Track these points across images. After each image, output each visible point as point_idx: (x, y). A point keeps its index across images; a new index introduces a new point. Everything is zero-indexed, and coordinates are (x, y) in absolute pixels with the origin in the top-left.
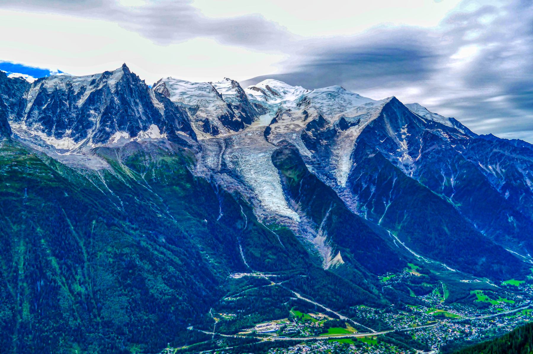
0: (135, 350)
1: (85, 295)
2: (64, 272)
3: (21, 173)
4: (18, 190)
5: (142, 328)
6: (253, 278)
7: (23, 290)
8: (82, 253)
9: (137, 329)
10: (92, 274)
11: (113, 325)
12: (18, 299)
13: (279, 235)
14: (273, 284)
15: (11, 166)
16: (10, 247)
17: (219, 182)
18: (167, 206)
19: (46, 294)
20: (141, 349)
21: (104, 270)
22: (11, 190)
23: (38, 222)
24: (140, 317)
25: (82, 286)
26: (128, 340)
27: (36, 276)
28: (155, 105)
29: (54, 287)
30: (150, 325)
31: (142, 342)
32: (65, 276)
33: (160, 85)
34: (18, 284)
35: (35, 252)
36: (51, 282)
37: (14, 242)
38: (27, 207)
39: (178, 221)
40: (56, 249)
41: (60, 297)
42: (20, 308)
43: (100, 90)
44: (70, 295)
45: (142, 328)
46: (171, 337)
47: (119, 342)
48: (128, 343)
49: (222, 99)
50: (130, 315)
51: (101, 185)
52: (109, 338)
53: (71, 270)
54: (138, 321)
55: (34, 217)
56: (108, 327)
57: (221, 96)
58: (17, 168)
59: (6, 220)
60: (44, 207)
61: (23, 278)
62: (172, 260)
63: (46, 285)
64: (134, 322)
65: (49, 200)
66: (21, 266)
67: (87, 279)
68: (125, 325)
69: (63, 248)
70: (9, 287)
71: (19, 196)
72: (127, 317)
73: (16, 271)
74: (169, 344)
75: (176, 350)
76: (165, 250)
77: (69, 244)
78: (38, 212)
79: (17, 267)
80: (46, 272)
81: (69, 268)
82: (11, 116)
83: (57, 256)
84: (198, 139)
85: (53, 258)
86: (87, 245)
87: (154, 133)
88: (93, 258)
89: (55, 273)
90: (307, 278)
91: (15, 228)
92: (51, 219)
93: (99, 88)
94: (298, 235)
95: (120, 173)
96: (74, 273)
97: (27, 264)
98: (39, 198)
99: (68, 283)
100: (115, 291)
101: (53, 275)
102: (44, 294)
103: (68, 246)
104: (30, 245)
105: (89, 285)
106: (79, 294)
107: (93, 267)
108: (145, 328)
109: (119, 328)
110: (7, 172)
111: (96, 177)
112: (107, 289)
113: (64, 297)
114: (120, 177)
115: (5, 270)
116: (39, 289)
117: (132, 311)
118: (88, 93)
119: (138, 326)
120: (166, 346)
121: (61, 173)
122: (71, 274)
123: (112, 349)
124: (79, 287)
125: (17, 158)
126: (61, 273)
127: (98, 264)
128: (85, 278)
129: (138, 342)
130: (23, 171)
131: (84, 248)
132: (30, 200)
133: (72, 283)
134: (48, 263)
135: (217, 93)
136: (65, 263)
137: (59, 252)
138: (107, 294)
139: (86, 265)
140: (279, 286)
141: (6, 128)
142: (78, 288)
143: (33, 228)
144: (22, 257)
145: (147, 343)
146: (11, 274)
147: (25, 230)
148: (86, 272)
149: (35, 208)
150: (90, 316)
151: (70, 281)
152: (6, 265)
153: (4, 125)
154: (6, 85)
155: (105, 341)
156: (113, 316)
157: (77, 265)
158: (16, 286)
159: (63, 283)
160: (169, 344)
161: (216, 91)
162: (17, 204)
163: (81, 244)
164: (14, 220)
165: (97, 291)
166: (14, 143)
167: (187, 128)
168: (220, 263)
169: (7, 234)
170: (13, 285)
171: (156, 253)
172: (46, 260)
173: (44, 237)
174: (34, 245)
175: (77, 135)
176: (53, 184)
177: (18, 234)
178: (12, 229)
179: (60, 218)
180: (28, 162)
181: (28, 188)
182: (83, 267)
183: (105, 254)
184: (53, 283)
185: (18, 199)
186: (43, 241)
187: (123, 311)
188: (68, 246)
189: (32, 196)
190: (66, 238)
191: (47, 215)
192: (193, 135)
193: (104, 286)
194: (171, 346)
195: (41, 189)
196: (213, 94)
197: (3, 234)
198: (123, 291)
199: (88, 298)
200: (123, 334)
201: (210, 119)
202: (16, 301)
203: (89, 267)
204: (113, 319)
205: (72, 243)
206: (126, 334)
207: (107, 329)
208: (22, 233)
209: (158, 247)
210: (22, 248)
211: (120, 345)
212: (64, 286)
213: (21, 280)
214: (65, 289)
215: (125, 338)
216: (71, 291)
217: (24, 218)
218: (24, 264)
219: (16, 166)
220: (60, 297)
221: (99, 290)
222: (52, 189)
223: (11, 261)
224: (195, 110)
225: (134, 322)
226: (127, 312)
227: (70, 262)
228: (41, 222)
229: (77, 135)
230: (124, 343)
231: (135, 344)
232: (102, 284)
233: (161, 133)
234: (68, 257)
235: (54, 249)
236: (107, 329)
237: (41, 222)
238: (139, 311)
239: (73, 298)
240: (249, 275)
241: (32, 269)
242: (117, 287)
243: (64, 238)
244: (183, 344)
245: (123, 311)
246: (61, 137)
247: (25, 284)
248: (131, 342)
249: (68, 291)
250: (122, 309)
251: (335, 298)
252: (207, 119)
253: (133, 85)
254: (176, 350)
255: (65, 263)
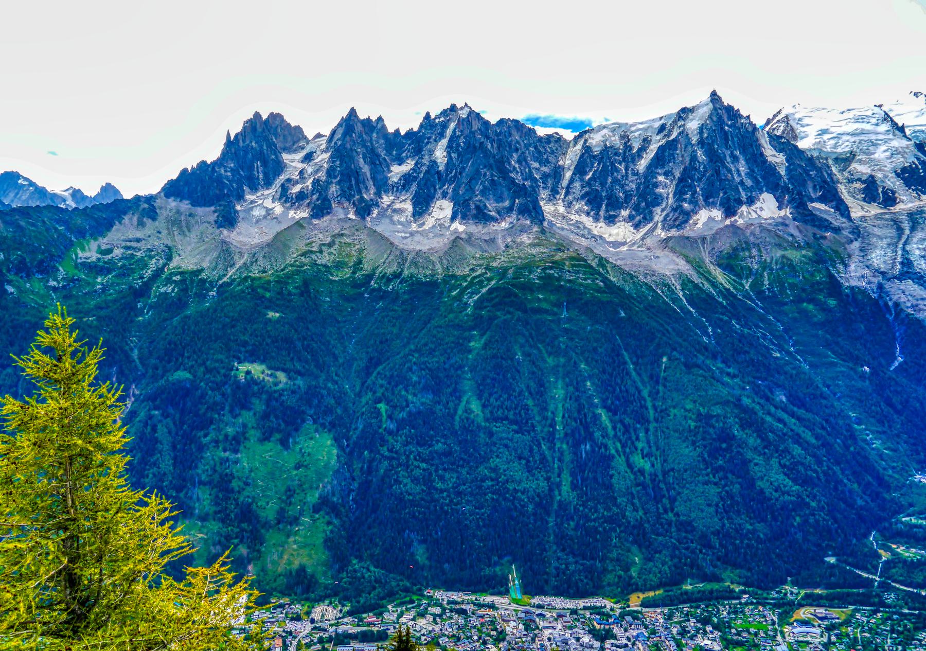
1: (650, 475)
2: (619, 434)
3: (558, 279)
4: (555, 305)
5: (742, 542)
7: (562, 454)
8: (647, 409)
9: (734, 544)
10: (662, 443)
11: (694, 529)
12: (556, 466)
15: (544, 269)
16: (545, 389)
17: (895, 298)
18: (791, 338)
19: (593, 464)
20: (740, 577)
21: (680, 438)
22: (545, 306)
23: (582, 353)
24: (740, 525)
25: (646, 459)
26: (719, 559)
27: (580, 435)
28: (769, 159)
29: (605, 456)
30: (756, 541)
31: (741, 567)
32: (620, 441)
33: (778, 121)
34: (555, 445)
35: (577, 399)
36: (600, 448)
37: (549, 382)
38: (566, 331)
39: (812, 365)
40: (607, 398)
41: (613, 472)
42: (558, 479)
43: (673, 140)
44: (628, 470)
45: (742, 542)
46: (793, 568)
48: (719, 563)
49: (905, 136)
50: (723, 518)
51: (676, 300)
52: (687, 549)
53: (630, 433)
54: (737, 531)
55: (577, 347)
56: (686, 532)
57: (902, 129)
58: (552, 272)
59: (538, 349)
60: (591, 331)
61: (562, 435)
62: (798, 435)
63: (593, 451)
64: (728, 531)
65: (597, 322)
66: (559, 419)
67: (654, 449)
68: (713, 533)
69: (618, 399)
70: (544, 447)
71: (555, 314)
72: (716, 519)
73: (553, 425)
74: (789, 579)
75: (803, 592)
77: (627, 391)
78: (582, 340)
79: (553, 419)
80: (594, 432)
81: (627, 428)
82: (544, 194)
83: (608, 409)
84: (853, 215)
85: (604, 410)
86: (654, 395)
87: (768, 208)
88: (662, 418)
89: (605, 435)
91: (550, 361)
92: (600, 350)
93: (671, 138)
95: (707, 279)
96: (634, 438)
97: (566, 415)
98: (583, 318)
99: (624, 453)
100: (699, 475)
101: (603, 437)
102: (590, 464)
103: (625, 394)
104: (571, 389)
105: (656, 459)
106: (642, 471)
107: (663, 432)
108: (747, 544)
109: (703, 536)
110: (539, 278)
111: (667, 286)
112: (686, 471)
113: (619, 473)
114: (707, 286)
115: (539, 422)
116: (584, 456)
117: (726, 512)
118: (653, 148)
119: (736, 539)
120: (784, 582)
121: (614, 280)
122: (630, 438)
123: (692, 568)
124: (642, 460)
125: (553, 256)
126: (615, 435)
127: (671, 427)
128: (650, 447)
129: (735, 565)
130: (561, 276)
131: (648, 399)
132: (569, 320)
133: (631, 453)
134: (596, 417)
135: (894, 124)
136: (621, 422)
137: (612, 403)
138: (685, 477)
139: (652, 426)
141: (537, 212)
142: (639, 461)
143: (575, 363)
144: (560, 405)
145: (749, 570)
146: (546, 430)
147: (564, 366)
148: (652, 438)
149: (577, 333)
150: (658, 509)
151: (628, 450)
152: (540, 414)
153: (534, 208)
154: (536, 148)
155: (681, 553)
156: (693, 515)
157: (638, 426)
158: (552, 448)
159: (617, 451)
160: (789, 579)
161: (892, 120)
162: (553, 326)
163: (645, 393)
164: (549, 349)
165: (669, 471)
166: (548, 235)
167: (831, 195)
169: (541, 369)
170: (548, 444)
171: (768, 419)
172: (594, 413)
173: (590, 377)
174: (577, 389)
175: (638, 218)
176: (605, 297)
177: (555, 370)
178: (545, 362)
179: (613, 350)
180: (567, 263)
181: (568, 303)
182: (647, 431)
183: (683, 411)
184: (603, 450)
185: (555, 318)
186: (589, 383)
187: (712, 510)
188: (625, 394)
189: (575, 313)
190: (622, 381)
191: (595, 345)
192: (842, 209)
193: (679, 463)
194: (794, 583)
195: (586, 304)
196: (884, 127)
197: (535, 369)
198: (711, 476)
199: (655, 480)
200: (709, 546)
201: (879, 175)
202: (554, 468)
203: (656, 431)
204: (694, 520)
205: (632, 390)
206: (715, 548)
208: (560, 369)
209: (773, 410)
210: (559, 392)
212: (620, 456)
213: (559, 439)
214: (620, 462)
215: (713, 553)
216: (630, 466)
217: (563, 347)
218: (563, 416)
219: (551, 268)
220: (613, 472)
221: (673, 470)
222: (602, 304)
223: (546, 409)
224: (846, 160)
225: (728, 531)
226: (717, 511)
227: (627, 420)
228: (586, 354)
229: (638, 218)
230: (711, 561)
231: (730, 568)
232: (677, 461)
233: (780, 208)
234: (625, 413)
235: (604, 396)
236: (684, 534)
237: (586, 354)
238: (738, 513)
239: (632, 477)
241: (573, 423)
242: (701, 470)
243: (619, 381)
244: (817, 586)
245: (712, 510)
246: (614, 223)
247: (565, 446)
248: (724, 563)
249: (625, 465)
250: (709, 505)
252: (872, 177)
253: (730, 126)
254: (803, 592)
255: (621, 422)
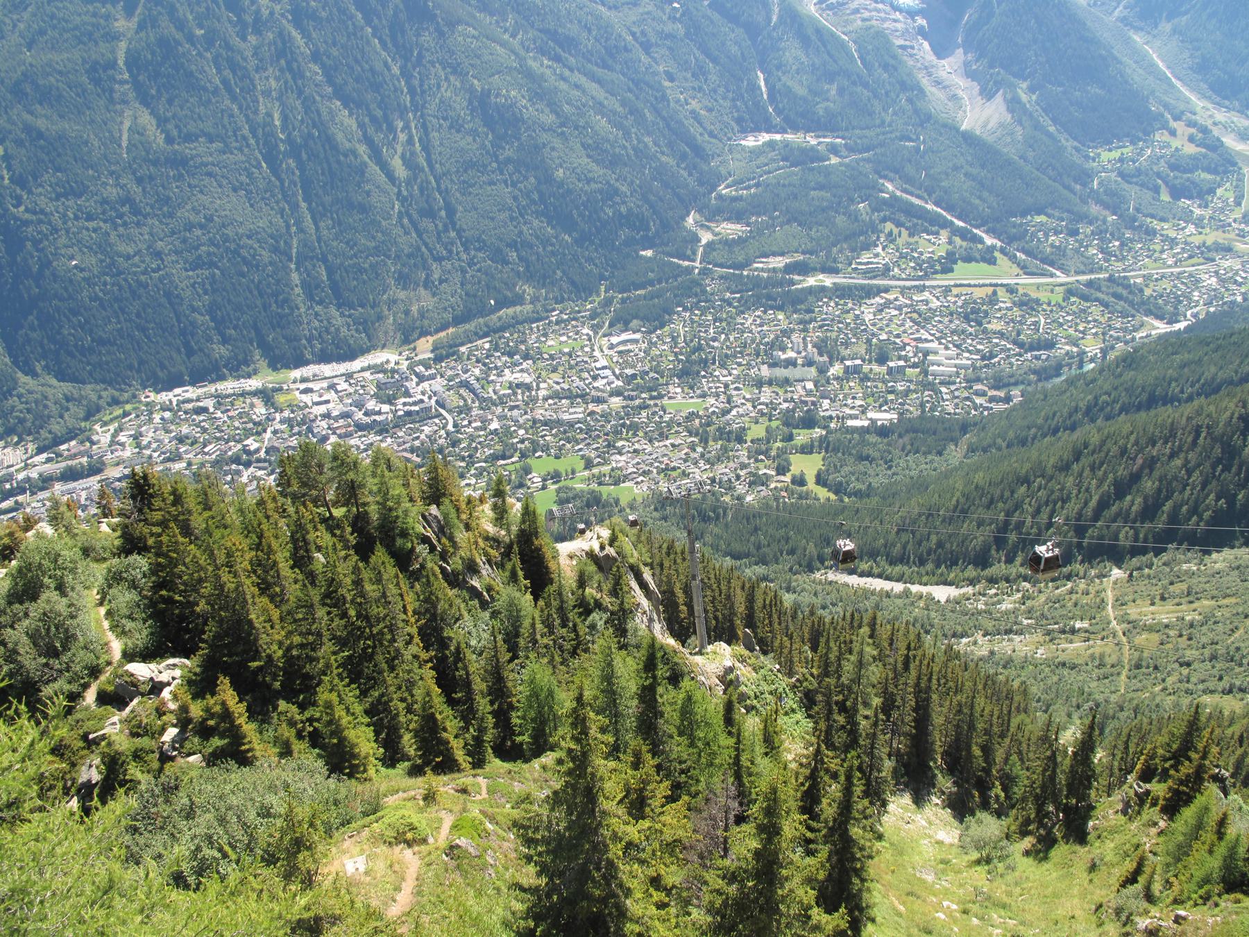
6: (786, 144)
13: (855, 42)
14: (834, 160)
36: (346, 156)
62: (601, 104)
76: (583, 80)
90: (917, 149)
94: (900, 42)
117: (522, 215)
140: (847, 166)
150: (436, 226)
168: (710, 110)
171: (563, 86)
209: (567, 73)
240: (778, 137)
245: (504, 216)
251: (980, 198)
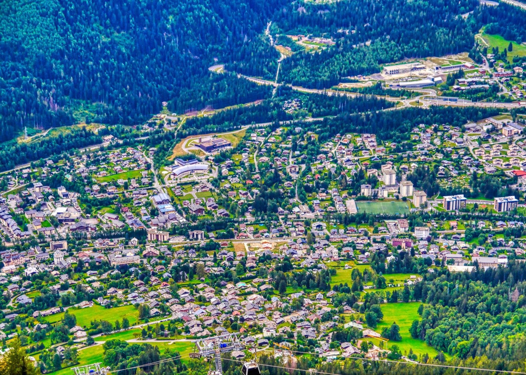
0: (83, 115)
5: (97, 63)
9: (84, 67)
11: (25, 54)
20: (98, 113)
24: (91, 38)
26: (66, 92)
30: (117, 59)
31: (99, 98)
45: (97, 63)
46: (169, 88)
47: (43, 95)
48: (67, 98)
50: (67, 30)
52: (18, 84)
54: (88, 47)
56: (14, 59)
64: (75, 49)
68: (54, 56)
72: (56, 35)
74: (165, 104)
75: (184, 118)
108: (105, 65)
109: (41, 62)
117: (70, 22)
119: (88, 60)
120: (158, 110)
123: (28, 111)
129: (91, 97)
145: (111, 100)
155: (9, 92)
156: (21, 33)
160: (165, 104)
187: (49, 21)
194: (172, 109)
200: (51, 76)
204: (24, 39)
206: (59, 77)
207: (11, 64)
211: (46, 103)
215: (58, 85)
225: (75, 49)
226: (56, 24)
230: (55, 96)
231: (83, 102)
236: (11, 64)
238: (88, 21)
244: (200, 106)
245: (49, 21)
248: (73, 97)
250: (43, 15)
254: (184, 118)
